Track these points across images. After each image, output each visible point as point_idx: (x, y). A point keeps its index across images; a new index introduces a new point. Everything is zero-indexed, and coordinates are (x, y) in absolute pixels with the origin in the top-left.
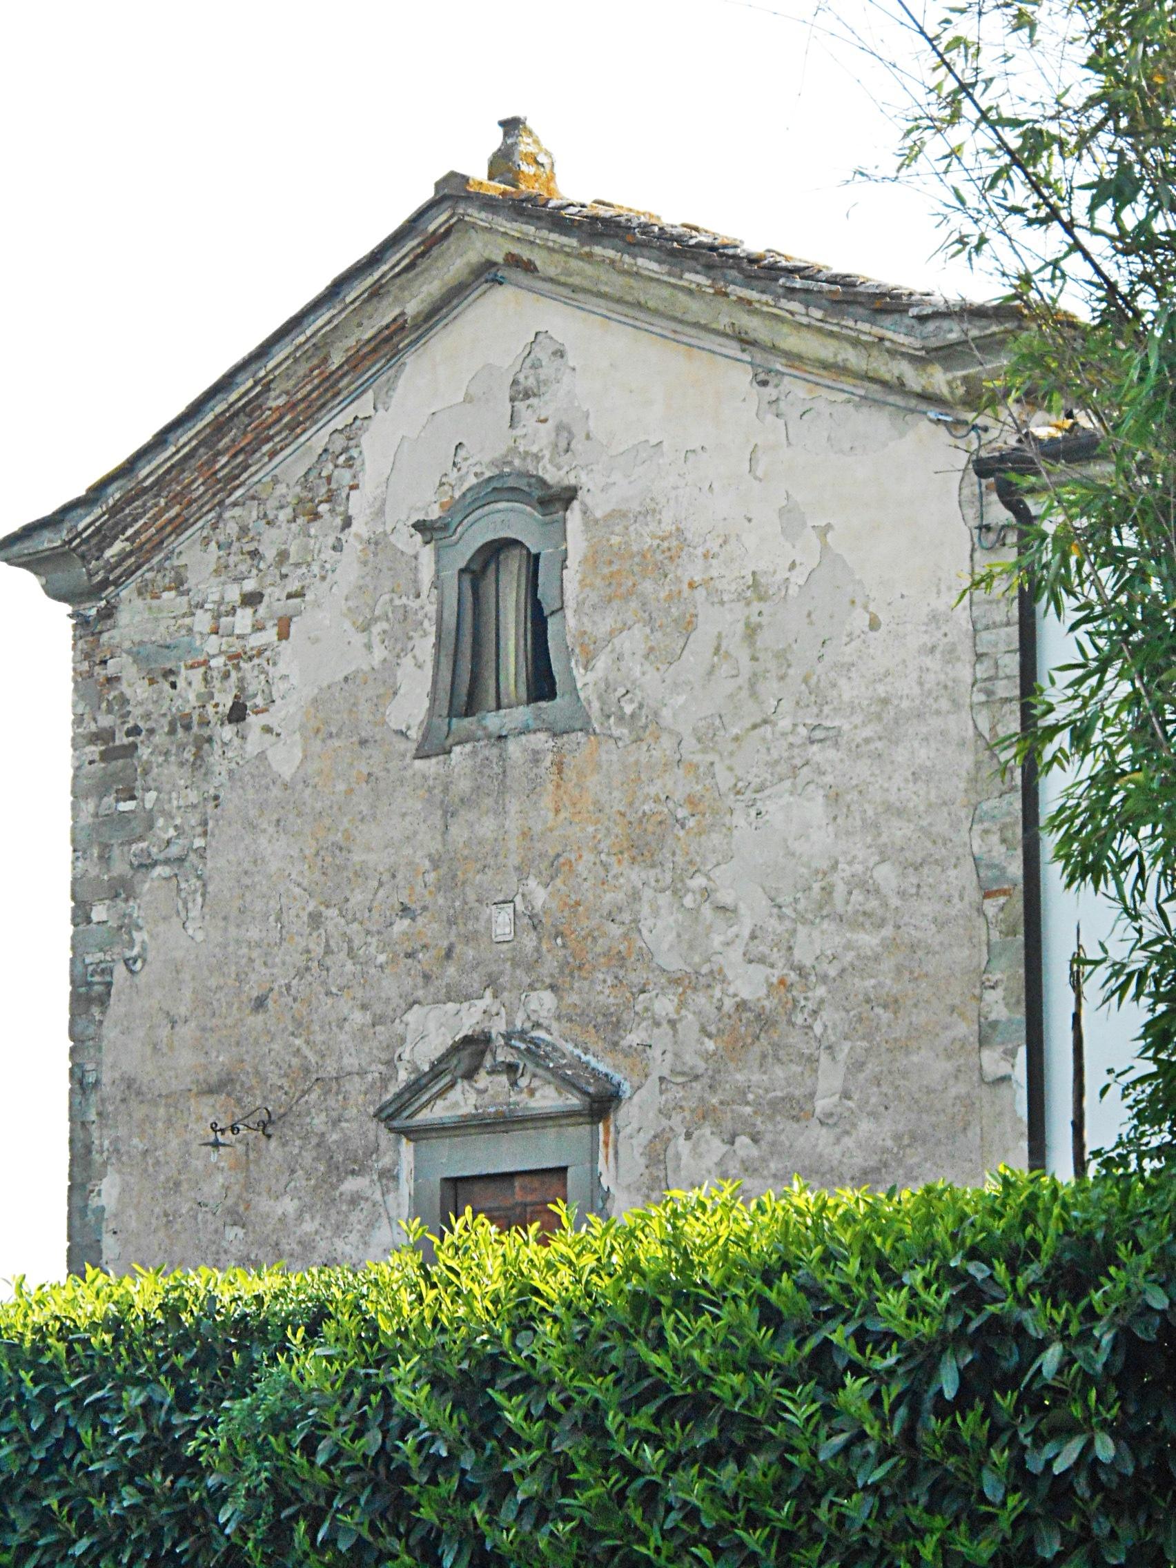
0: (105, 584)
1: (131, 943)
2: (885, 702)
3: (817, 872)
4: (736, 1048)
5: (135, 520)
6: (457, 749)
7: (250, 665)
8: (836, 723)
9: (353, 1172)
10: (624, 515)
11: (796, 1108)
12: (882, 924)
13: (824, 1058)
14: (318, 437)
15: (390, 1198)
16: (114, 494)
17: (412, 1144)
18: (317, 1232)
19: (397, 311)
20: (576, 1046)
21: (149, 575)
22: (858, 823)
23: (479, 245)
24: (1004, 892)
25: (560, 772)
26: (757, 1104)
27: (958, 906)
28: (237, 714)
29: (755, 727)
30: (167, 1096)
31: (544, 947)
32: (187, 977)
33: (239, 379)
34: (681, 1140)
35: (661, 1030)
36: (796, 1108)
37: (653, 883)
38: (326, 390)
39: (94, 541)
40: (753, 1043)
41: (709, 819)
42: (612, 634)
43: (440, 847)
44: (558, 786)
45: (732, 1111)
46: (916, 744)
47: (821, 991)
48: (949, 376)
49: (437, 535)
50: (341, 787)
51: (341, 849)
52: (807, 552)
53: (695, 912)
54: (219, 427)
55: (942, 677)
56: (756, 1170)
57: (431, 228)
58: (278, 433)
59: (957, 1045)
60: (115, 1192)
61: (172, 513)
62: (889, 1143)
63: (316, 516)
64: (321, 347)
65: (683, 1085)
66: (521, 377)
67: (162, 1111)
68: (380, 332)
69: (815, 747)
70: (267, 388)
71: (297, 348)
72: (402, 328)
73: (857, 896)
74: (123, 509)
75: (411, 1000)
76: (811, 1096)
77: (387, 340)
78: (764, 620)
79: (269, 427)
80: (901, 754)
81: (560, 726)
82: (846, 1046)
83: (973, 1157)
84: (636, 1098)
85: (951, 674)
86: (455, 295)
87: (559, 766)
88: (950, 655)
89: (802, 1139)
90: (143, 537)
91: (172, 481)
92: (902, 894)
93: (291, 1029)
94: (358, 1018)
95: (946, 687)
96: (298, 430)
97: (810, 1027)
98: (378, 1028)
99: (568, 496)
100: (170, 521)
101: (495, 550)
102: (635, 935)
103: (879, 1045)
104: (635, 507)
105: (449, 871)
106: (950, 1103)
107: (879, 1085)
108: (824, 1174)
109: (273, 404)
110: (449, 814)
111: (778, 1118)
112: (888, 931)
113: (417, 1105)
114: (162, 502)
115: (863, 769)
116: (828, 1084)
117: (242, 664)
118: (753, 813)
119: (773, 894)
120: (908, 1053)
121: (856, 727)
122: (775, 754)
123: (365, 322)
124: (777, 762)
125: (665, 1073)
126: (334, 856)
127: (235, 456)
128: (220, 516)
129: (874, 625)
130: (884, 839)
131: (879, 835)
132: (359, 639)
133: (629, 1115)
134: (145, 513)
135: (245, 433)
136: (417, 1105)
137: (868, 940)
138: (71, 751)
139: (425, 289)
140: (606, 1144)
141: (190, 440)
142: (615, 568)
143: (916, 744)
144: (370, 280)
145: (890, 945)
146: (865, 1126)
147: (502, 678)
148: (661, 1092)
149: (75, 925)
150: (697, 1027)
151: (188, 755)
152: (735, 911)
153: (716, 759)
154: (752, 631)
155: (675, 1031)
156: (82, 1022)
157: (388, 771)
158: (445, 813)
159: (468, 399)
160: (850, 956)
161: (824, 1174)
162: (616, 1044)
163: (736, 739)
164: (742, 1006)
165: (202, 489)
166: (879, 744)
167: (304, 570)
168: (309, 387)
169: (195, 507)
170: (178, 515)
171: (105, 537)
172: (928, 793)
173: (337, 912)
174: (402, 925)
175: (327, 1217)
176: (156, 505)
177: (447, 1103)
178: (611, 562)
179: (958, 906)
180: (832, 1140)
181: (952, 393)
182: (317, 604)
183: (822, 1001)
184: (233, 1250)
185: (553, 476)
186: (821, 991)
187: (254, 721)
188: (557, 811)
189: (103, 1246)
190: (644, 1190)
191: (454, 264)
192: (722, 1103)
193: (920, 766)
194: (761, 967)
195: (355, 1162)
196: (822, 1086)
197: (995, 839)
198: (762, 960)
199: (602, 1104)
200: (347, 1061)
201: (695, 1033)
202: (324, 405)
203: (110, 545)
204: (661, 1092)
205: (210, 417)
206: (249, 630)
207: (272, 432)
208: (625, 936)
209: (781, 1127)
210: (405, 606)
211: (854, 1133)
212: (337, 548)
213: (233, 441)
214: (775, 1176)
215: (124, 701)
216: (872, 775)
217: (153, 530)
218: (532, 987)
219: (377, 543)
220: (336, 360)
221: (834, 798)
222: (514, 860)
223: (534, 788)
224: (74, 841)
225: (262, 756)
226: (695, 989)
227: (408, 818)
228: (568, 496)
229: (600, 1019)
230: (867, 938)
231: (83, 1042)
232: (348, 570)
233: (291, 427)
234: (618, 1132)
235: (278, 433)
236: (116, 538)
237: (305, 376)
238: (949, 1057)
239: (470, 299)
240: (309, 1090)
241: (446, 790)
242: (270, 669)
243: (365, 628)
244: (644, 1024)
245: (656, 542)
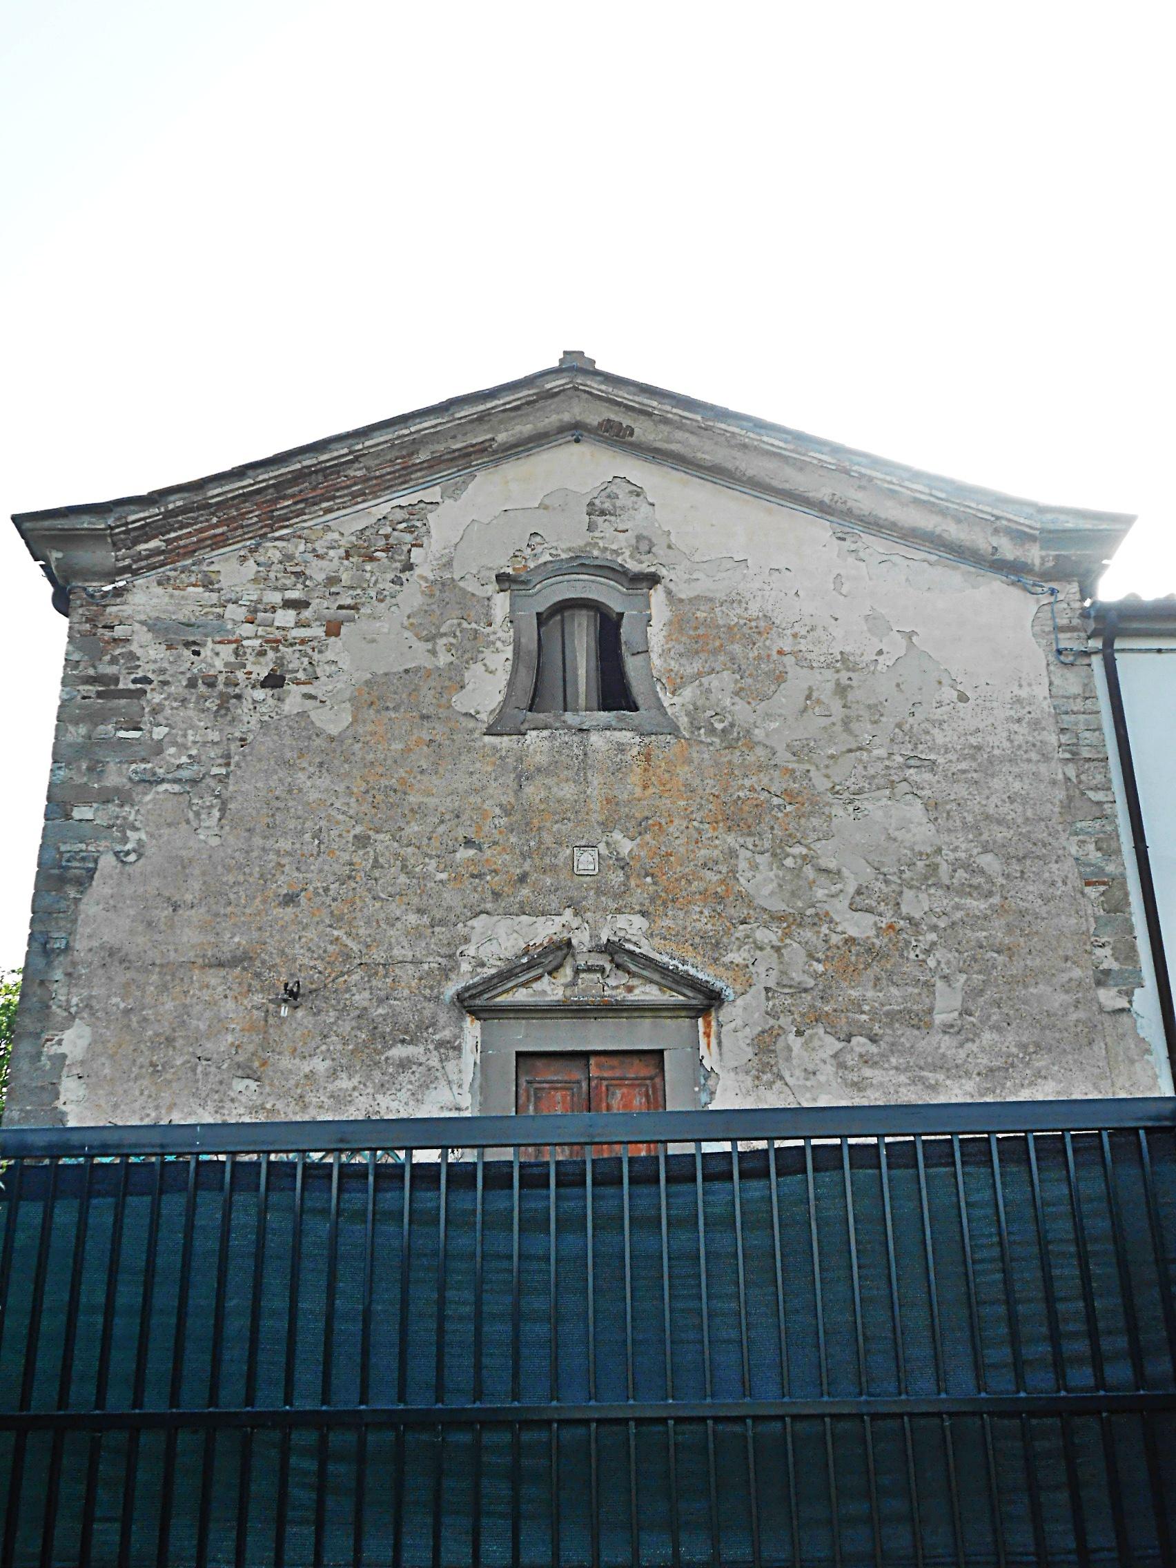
0: (127, 569)
1: (125, 840)
2: (979, 748)
3: (921, 854)
4: (850, 972)
5: (181, 528)
6: (534, 733)
7: (290, 650)
8: (932, 757)
9: (403, 1041)
10: (711, 600)
11: (920, 1020)
12: (990, 894)
13: (940, 984)
15: (451, 1066)
16: (176, 502)
17: (478, 1024)
18: (354, 1089)
19: (489, 436)
20: (672, 958)
21: (172, 574)
22: (958, 823)
23: (576, 410)
24: (1104, 883)
25: (648, 759)
26: (873, 1014)
27: (1060, 889)
28: (274, 681)
29: (850, 751)
30: (162, 966)
31: (633, 883)
32: (197, 872)
33: (332, 446)
34: (792, 1037)
35: (765, 952)
36: (920, 1020)
37: (751, 847)
38: (396, 478)
39: (133, 534)
40: (866, 969)
41: (807, 808)
42: (699, 675)
43: (513, 800)
44: (645, 770)
45: (847, 1018)
46: (1010, 779)
47: (932, 937)
48: (1044, 553)
49: (514, 587)
50: (397, 746)
51: (395, 791)
52: (895, 647)
53: (797, 872)
54: (299, 476)
55: (1031, 739)
56: (876, 1063)
57: (548, 386)
58: (340, 497)
59: (1074, 984)
60: (84, 1043)
61: (219, 531)
62: (1014, 1050)
63: (372, 559)
64: (418, 443)
65: (792, 995)
66: (597, 502)
67: (155, 978)
68: (465, 447)
69: (912, 771)
70: (356, 459)
71: (399, 437)
72: (485, 450)
73: (961, 873)
74: (177, 516)
75: (478, 910)
76: (930, 1011)
77: (469, 455)
78: (854, 683)
79: (338, 490)
80: (996, 783)
81: (648, 728)
82: (963, 978)
83: (1101, 1064)
84: (739, 1002)
85: (1039, 738)
86: (540, 440)
88: (1036, 725)
89: (924, 1042)
90: (182, 543)
91: (233, 506)
92: (1007, 876)
93: (328, 922)
94: (412, 918)
95: (1034, 745)
96: (359, 499)
97: (924, 961)
98: (437, 929)
99: (653, 580)
100: (215, 536)
101: (565, 607)
102: (732, 882)
103: (996, 979)
104: (721, 596)
105: (522, 819)
106: (1071, 1024)
107: (999, 1007)
108: (948, 1070)
109: (351, 473)
110: (522, 778)
111: (897, 1025)
112: (996, 900)
113: (500, 990)
114: (215, 520)
115: (961, 790)
116: (946, 1005)
117: (281, 647)
118: (851, 808)
119: (876, 865)
120: (1026, 986)
121: (950, 761)
122: (872, 771)
123: (459, 436)
124: (874, 777)
125: (772, 984)
126: (387, 796)
127: (295, 503)
128: (258, 545)
129: (963, 698)
130: (985, 837)
131: (981, 834)
133: (733, 1014)
134: (192, 525)
135: (314, 489)
136: (500, 990)
137: (978, 905)
138: (60, 687)
139: (518, 428)
140: (707, 1035)
141: (270, 479)
142: (700, 632)
143: (1010, 779)
144: (482, 408)
145: (999, 911)
146: (988, 1037)
147: (569, 690)
148: (768, 999)
149: (47, 819)
150: (803, 953)
151: (212, 705)
152: (839, 872)
153: (813, 768)
154: (842, 690)
155: (781, 956)
156: (48, 900)
157: (453, 740)
158: (519, 777)
159: (543, 506)
160: (959, 915)
161: (948, 1070)
162: (716, 960)
163: (832, 757)
164: (850, 941)
165: (255, 519)
166: (975, 775)
167: (359, 591)
168: (389, 470)
169: (240, 532)
170: (222, 534)
171: (146, 534)
172: (1024, 811)
173: (388, 837)
174: (464, 854)
175: (369, 1077)
176: (207, 521)
177: (530, 990)
178: (696, 628)
179: (1060, 889)
180: (955, 1044)
181: (1042, 564)
182: (373, 617)
183: (934, 944)
184: (243, 1099)
185: (633, 566)
186: (932, 937)
187: (294, 692)
188: (645, 787)
189: (62, 1089)
190: (754, 1072)
191: (551, 418)
192: (835, 1011)
193: (1015, 793)
194: (868, 915)
195: (406, 1033)
196: (939, 1004)
197: (1092, 847)
198: (869, 910)
199: (711, 1000)
200: (397, 952)
201: (802, 956)
202: (391, 486)
203: (146, 542)
204: (768, 999)
205: (298, 466)
206: (292, 625)
207: (338, 494)
208: (722, 882)
209: (899, 1032)
210: (476, 631)
211: (978, 1041)
212: (397, 581)
213: (301, 491)
214: (897, 1069)
215: (132, 656)
216: (970, 794)
217: (195, 539)
218: (619, 911)
219: (443, 584)
220: (423, 456)
221: (932, 806)
222: (595, 817)
223: (619, 770)
224: (54, 754)
225: (303, 714)
226: (800, 925)
227: (475, 777)
228: (653, 580)
229: (697, 940)
230: (975, 903)
231: (42, 914)
232: (412, 597)
233: (354, 496)
234: (720, 1025)
235: (340, 497)
236: (155, 537)
237: (391, 461)
238: (1067, 992)
239: (560, 441)
240: (349, 972)
241: (520, 760)
242: (316, 656)
243: (430, 639)
244: (747, 947)
245: (742, 622)
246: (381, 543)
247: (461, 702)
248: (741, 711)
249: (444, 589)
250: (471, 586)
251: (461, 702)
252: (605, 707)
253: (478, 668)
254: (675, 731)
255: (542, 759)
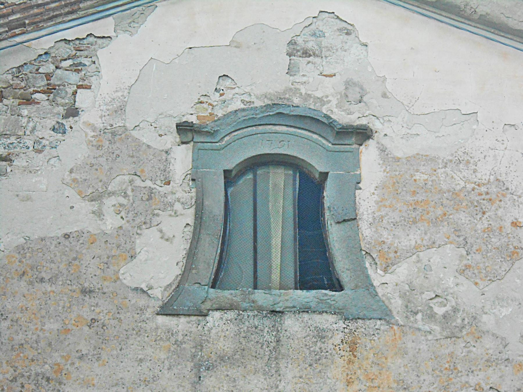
10: (433, 160)
14: (45, 41)
25: (353, 350)
42: (417, 248)
44: (350, 362)
49: (197, 138)
50: (53, 326)
51: (48, 380)
63: (28, 101)
66: (300, 40)
81: (354, 311)
87: (353, 347)
96: (17, 31)
99: (363, 134)
132: (85, 207)
157: (120, 320)
158: (198, 367)
159: (235, 44)
167: (13, 139)
178: (414, 193)
182: (28, 170)
185: (342, 117)
202: (56, 16)
219: (114, 134)
227: (146, 365)
228: (363, 134)
241: (199, 346)
243: (96, 198)
245: (470, 186)
246: (42, 83)
247: (131, 275)
248: (467, 294)
249: (113, 138)
250: (147, 137)
251: (131, 275)
252: (304, 283)
253: (151, 235)
254: (386, 315)
255: (225, 346)
